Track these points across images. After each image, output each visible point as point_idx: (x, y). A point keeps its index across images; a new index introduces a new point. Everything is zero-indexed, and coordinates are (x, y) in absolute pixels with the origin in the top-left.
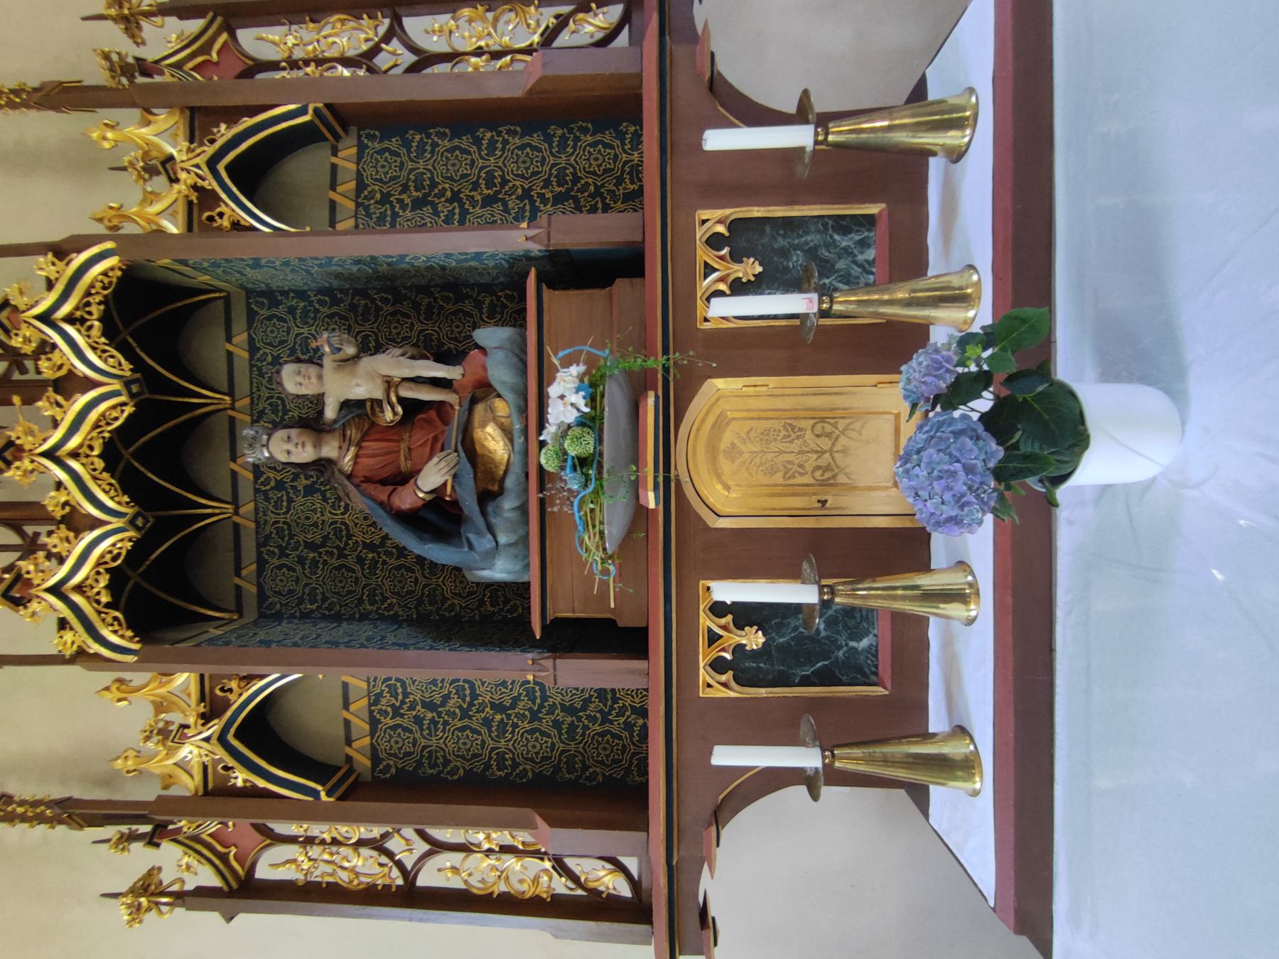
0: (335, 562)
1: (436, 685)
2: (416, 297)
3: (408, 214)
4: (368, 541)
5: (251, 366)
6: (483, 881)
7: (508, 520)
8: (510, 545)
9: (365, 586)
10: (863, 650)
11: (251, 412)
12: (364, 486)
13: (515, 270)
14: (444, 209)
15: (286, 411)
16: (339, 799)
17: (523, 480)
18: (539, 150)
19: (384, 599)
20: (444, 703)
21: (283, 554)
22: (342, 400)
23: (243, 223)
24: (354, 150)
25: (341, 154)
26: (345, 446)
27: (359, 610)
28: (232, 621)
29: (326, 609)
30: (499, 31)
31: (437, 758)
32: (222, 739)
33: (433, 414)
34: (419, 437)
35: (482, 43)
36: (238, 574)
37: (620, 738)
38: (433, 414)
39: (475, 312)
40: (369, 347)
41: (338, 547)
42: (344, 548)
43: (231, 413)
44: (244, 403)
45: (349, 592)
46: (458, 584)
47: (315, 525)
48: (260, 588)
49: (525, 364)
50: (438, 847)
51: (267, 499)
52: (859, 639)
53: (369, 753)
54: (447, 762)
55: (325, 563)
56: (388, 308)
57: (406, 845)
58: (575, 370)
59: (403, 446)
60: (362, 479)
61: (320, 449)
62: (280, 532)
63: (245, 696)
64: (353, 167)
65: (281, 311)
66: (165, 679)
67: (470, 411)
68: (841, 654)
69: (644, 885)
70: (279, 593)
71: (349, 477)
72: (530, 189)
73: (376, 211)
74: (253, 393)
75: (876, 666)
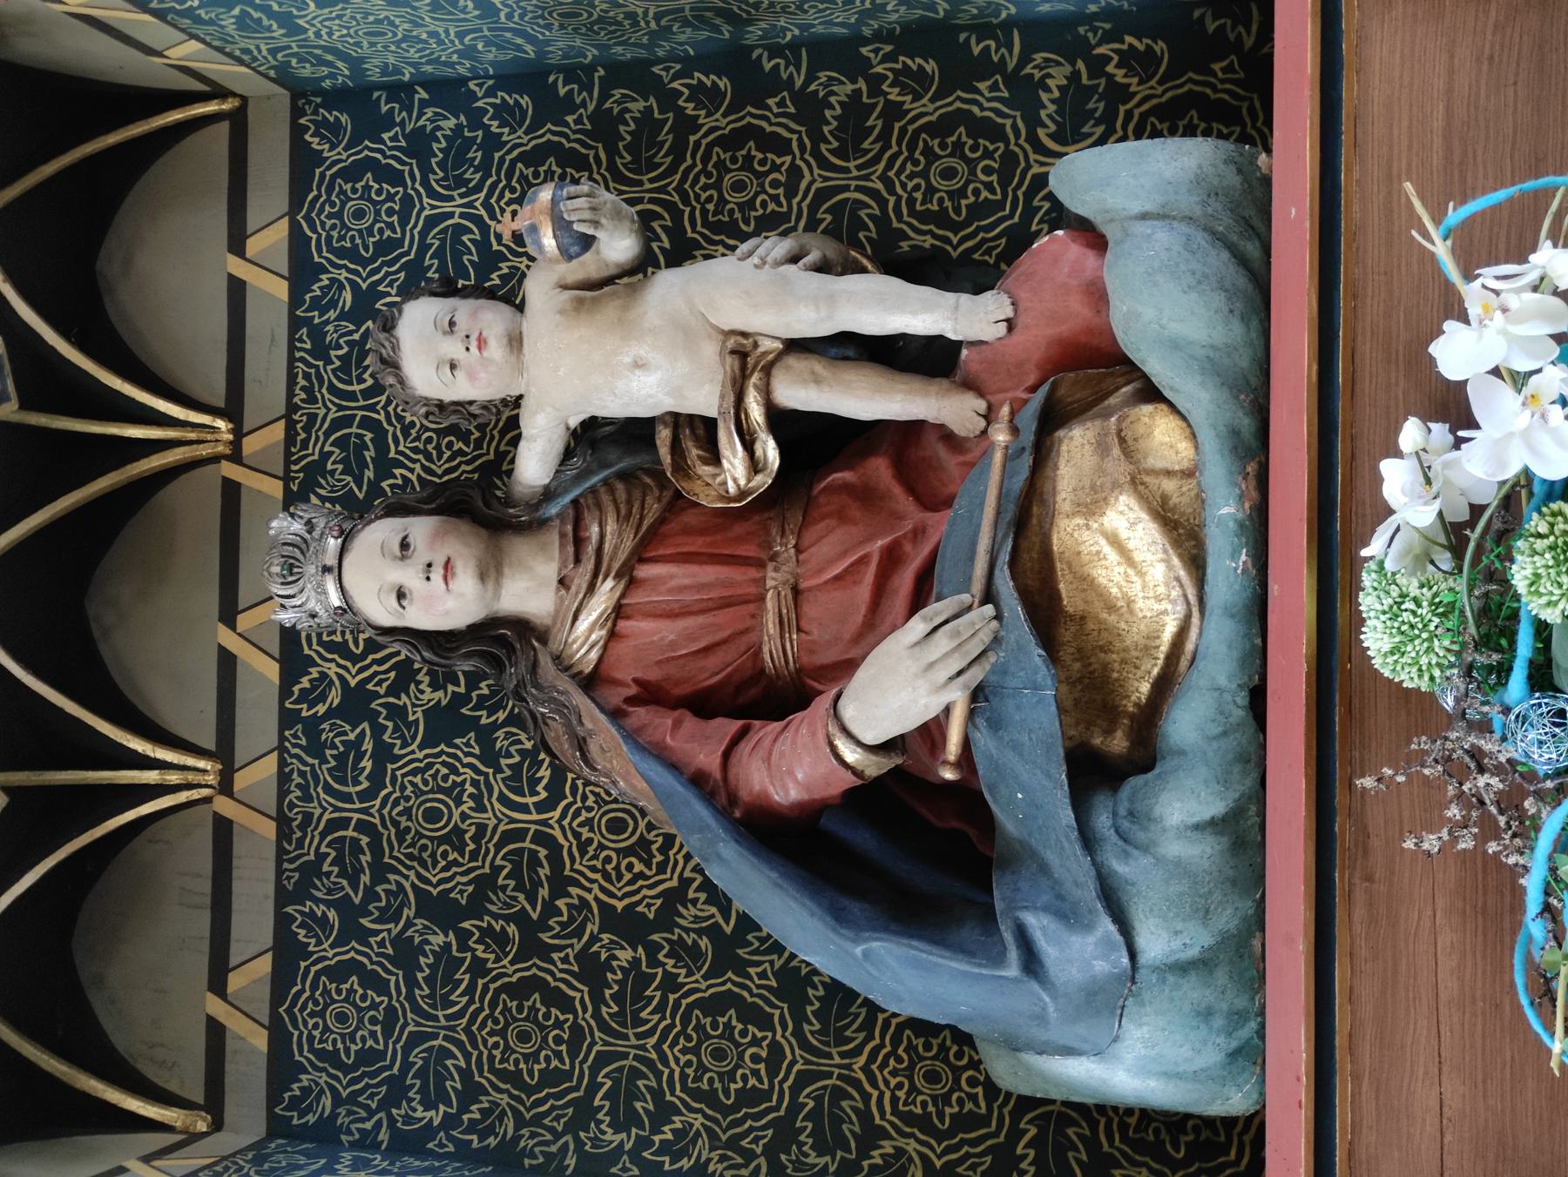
2: (810, 78)
4: (620, 905)
9: (603, 1059)
11: (287, 470)
19: (664, 1113)
21: (352, 932)
22: (574, 422)
27: (579, 1144)
28: (193, 1137)
29: (472, 1127)
36: (218, 985)
41: (521, 918)
42: (543, 925)
43: (229, 470)
44: (266, 440)
45: (551, 1077)
46: (919, 1082)
47: (455, 838)
51: (316, 748)
55: (479, 968)
59: (774, 578)
60: (633, 690)
61: (498, 584)
62: (347, 854)
70: (332, 1058)
74: (295, 408)
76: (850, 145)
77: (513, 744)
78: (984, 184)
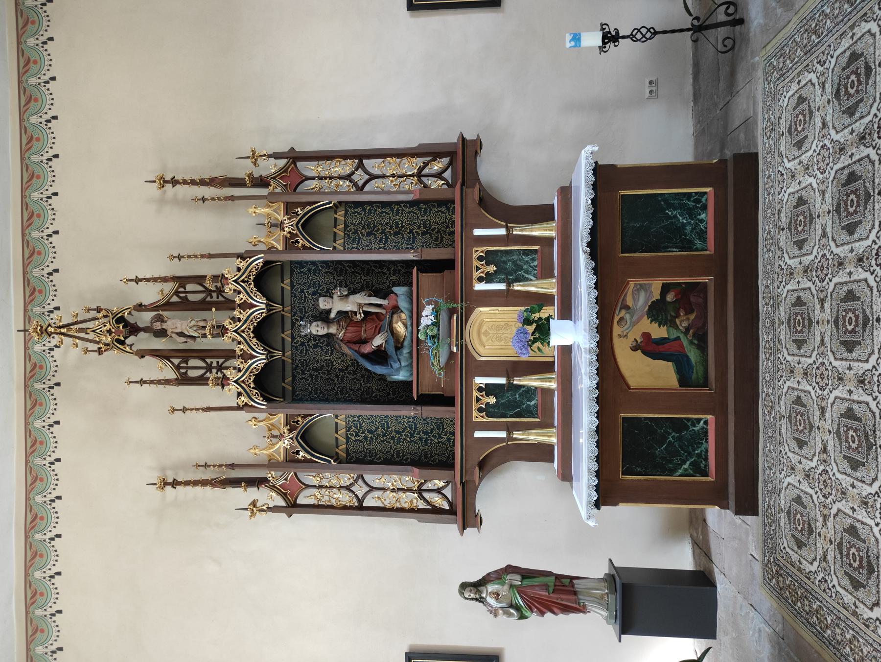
0: (326, 377)
3: (365, 238)
5: (291, 293)
7: (405, 357)
8: (405, 366)
9: (339, 387)
10: (533, 405)
12: (348, 344)
13: (408, 265)
14: (379, 236)
15: (306, 312)
16: (338, 463)
17: (410, 342)
18: (416, 214)
20: (376, 430)
21: (303, 373)
23: (306, 245)
24: (343, 212)
26: (340, 329)
28: (282, 401)
30: (402, 168)
31: (372, 453)
32: (296, 438)
34: (369, 326)
35: (395, 172)
37: (445, 444)
38: (374, 316)
39: (387, 272)
40: (354, 292)
41: (327, 370)
42: (330, 371)
43: (282, 313)
45: (332, 390)
47: (318, 361)
48: (293, 387)
50: (372, 489)
54: (376, 455)
55: (322, 377)
56: (350, 270)
57: (360, 490)
62: (302, 364)
63: (305, 422)
64: (343, 219)
65: (305, 270)
66: (271, 417)
67: (392, 317)
68: (524, 406)
70: (301, 390)
71: (341, 341)
72: (413, 229)
73: (352, 236)
75: (537, 411)
76: (368, 274)
77: (325, 348)
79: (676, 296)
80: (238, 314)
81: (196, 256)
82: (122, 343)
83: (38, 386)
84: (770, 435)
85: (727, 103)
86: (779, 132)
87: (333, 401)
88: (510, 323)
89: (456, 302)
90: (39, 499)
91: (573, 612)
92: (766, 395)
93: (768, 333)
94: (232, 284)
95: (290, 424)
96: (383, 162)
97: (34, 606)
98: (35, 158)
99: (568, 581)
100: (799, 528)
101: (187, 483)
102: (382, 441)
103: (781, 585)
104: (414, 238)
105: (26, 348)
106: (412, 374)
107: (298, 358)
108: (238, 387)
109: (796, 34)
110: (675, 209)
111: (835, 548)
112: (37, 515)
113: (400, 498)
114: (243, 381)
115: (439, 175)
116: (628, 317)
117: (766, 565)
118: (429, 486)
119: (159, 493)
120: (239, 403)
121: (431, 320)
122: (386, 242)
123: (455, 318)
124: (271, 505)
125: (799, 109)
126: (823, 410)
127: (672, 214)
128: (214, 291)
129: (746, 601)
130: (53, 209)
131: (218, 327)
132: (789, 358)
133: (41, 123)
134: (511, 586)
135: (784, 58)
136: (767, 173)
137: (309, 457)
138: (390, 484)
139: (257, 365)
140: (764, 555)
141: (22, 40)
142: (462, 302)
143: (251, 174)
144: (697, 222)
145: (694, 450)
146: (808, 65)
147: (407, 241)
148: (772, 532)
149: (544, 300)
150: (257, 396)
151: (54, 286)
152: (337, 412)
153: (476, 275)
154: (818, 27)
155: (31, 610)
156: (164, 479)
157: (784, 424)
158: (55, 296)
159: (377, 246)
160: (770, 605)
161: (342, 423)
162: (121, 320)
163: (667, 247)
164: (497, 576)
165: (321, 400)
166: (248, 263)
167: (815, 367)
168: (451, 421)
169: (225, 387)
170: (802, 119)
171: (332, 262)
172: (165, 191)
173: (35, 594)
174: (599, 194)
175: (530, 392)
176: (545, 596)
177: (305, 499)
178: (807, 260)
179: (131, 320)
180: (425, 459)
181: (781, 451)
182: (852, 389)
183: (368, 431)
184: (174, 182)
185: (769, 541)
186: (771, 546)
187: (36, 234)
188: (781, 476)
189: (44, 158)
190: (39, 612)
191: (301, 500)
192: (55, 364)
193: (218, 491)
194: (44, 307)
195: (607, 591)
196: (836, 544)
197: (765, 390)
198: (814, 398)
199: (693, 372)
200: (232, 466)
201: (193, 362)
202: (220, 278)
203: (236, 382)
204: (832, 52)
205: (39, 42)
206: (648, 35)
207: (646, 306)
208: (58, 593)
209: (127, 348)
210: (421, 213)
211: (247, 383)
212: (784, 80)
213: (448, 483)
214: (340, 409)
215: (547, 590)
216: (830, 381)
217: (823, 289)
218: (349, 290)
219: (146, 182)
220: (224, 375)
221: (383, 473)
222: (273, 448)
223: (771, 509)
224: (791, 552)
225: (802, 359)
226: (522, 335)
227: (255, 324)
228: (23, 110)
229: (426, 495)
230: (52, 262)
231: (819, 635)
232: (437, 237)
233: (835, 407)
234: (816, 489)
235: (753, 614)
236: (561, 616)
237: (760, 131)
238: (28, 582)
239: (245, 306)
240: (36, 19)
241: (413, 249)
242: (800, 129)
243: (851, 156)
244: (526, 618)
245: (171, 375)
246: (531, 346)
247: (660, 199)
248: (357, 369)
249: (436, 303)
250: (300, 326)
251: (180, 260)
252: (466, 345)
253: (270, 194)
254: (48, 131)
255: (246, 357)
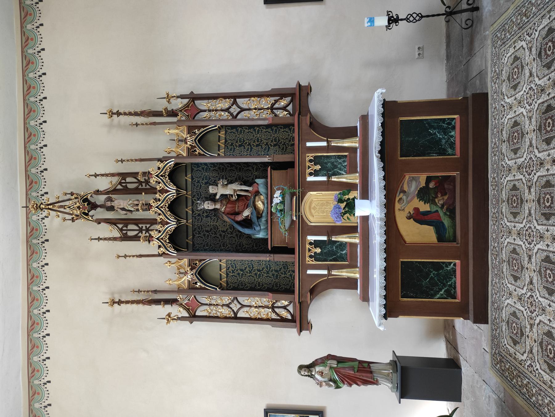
1: (243, 265)
5: (192, 183)
6: (254, 315)
8: (264, 229)
12: (227, 215)
13: (265, 164)
14: (246, 147)
18: (270, 133)
20: (245, 269)
21: (199, 233)
23: (201, 153)
24: (224, 132)
25: (221, 133)
28: (186, 251)
32: (195, 274)
33: (244, 198)
34: (240, 204)
35: (256, 107)
37: (289, 278)
38: (244, 198)
40: (231, 182)
41: (214, 232)
42: (216, 232)
43: (186, 195)
45: (217, 244)
47: (208, 226)
48: (193, 242)
49: (267, 187)
50: (243, 306)
52: (343, 251)
53: (226, 282)
54: (245, 285)
55: (211, 236)
57: (235, 306)
58: (279, 192)
63: (201, 264)
64: (224, 136)
65: (200, 168)
67: (255, 198)
69: (294, 315)
71: (223, 213)
72: (268, 143)
73: (230, 147)
75: (347, 257)
78: (250, 175)
79: (435, 184)
80: (158, 196)
81: (132, 160)
82: (87, 214)
83: (35, 241)
84: (496, 273)
85: (468, 61)
86: (502, 79)
87: (218, 251)
88: (330, 202)
89: (295, 188)
90: (36, 312)
91: (370, 384)
92: (494, 247)
93: (495, 208)
94: (155, 178)
95: (191, 265)
96: (249, 100)
97: (33, 378)
98: (32, 99)
99: (367, 364)
100: (515, 332)
101: (127, 302)
102: (249, 276)
103: (503, 368)
104: (269, 148)
105: (27, 218)
106: (267, 234)
107: (196, 224)
108: (159, 242)
109: (513, 16)
110: (435, 129)
111: (538, 345)
112: (34, 369)
113: (260, 312)
114: (162, 239)
115: (284, 108)
116: (404, 197)
117: (493, 356)
118: (279, 304)
119: (110, 308)
120: (160, 252)
121: (280, 200)
122: (251, 151)
123: (295, 198)
124: (180, 316)
125: (515, 65)
126: (530, 257)
127: (433, 132)
128: (143, 182)
129: (480, 378)
130: (43, 131)
131: (146, 204)
132: (508, 224)
133: (35, 77)
134: (331, 368)
135: (505, 32)
136: (494, 105)
137: (203, 286)
138: (254, 303)
139: (171, 228)
140: (492, 349)
141: (24, 26)
142: (299, 188)
143: (166, 108)
144: (449, 137)
145: (447, 282)
146: (520, 36)
147: (264, 150)
148: (497, 335)
149: (351, 187)
150: (170, 248)
151: (44, 179)
152: (220, 258)
153: (308, 171)
154: (527, 12)
155: (31, 381)
156: (113, 300)
157: (505, 266)
158: (45, 185)
159: (245, 153)
160: (495, 381)
161: (224, 265)
162: (86, 200)
163: (430, 153)
164: (322, 361)
165: (210, 250)
166: (165, 164)
167: (525, 229)
168: (293, 263)
169: (151, 242)
170: (517, 71)
171: (217, 163)
172: (113, 120)
173: (34, 371)
174: (386, 119)
175: (342, 245)
176: (352, 374)
177: (201, 312)
178: (520, 161)
179: (92, 200)
180: (276, 287)
181: (503, 283)
182: (549, 244)
183: (241, 270)
184: (118, 114)
185: (495, 340)
186: (496, 343)
187: (33, 147)
188: (503, 299)
189: (38, 100)
190: (36, 382)
191: (198, 313)
192: (45, 228)
193: (147, 307)
194: (38, 192)
195: (391, 371)
196: (539, 342)
197: (493, 244)
198: (524, 249)
199: (446, 233)
200: (155, 292)
201: (130, 227)
202: (147, 174)
203: (157, 239)
204: (536, 28)
205: (34, 27)
206: (418, 18)
207: (415, 192)
208: (48, 370)
209: (90, 218)
210: (273, 132)
211: (164, 240)
212: (505, 46)
213: (290, 302)
214: (223, 256)
215: (353, 370)
216: (535, 239)
217: (530, 180)
218: (228, 181)
219: (101, 114)
220: (150, 235)
221: (250, 296)
222: (181, 280)
223: (496, 320)
224: (509, 347)
225: (517, 225)
226: (337, 209)
227: (169, 203)
228: (24, 69)
229: (276, 310)
230: (43, 164)
231: (528, 400)
232: (283, 148)
233: (538, 255)
234: (525, 307)
235: (485, 386)
236: (363, 387)
237: (489, 79)
238: (30, 363)
239: (163, 191)
240: (32, 12)
241: (268, 155)
242: (515, 77)
243: (549, 95)
244: (340, 388)
245: (117, 234)
246: (343, 216)
247: (425, 122)
248: (233, 231)
249: (283, 189)
250: (197, 204)
251: (122, 163)
252: (302, 216)
253: (178, 121)
254: (40, 82)
255: (163, 223)
